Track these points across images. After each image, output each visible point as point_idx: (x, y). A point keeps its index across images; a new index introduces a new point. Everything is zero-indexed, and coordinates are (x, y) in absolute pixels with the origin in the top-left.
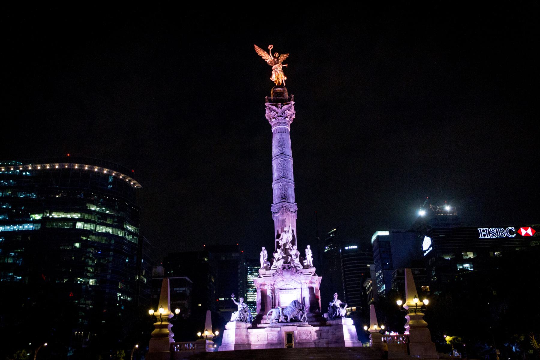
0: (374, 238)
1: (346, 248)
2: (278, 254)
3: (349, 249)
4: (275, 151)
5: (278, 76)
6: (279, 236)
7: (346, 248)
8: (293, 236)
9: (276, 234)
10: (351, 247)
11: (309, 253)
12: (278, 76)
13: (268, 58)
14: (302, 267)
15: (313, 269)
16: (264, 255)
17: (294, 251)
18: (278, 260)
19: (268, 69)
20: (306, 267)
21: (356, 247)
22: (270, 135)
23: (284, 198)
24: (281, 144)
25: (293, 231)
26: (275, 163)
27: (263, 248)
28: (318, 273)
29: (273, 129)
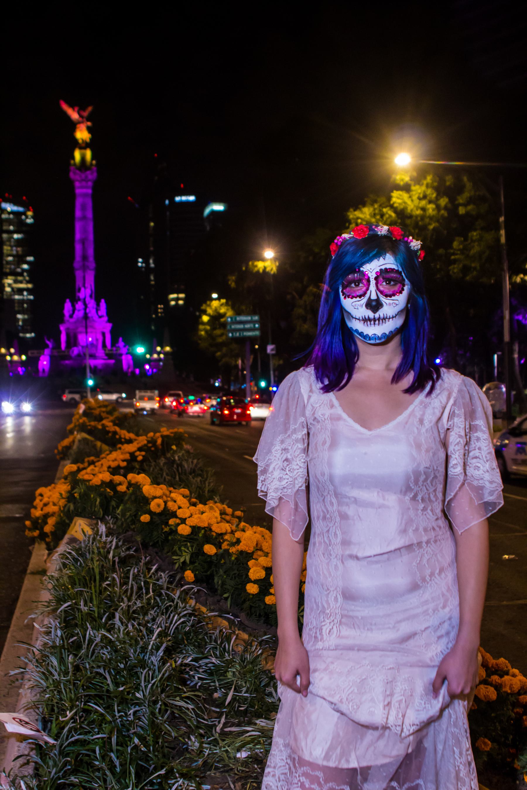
0: (207, 211)
1: (178, 199)
2: (79, 305)
3: (182, 203)
4: (78, 213)
5: (82, 134)
6: (79, 290)
7: (178, 199)
8: (92, 290)
9: (77, 288)
10: (184, 198)
11: (103, 304)
12: (82, 134)
13: (75, 116)
14: (97, 316)
15: (106, 319)
16: (68, 305)
17: (91, 303)
18: (79, 310)
19: (73, 126)
20: (100, 317)
21: (192, 198)
22: (73, 196)
23: (85, 258)
24: (84, 208)
25: (91, 286)
26: (78, 226)
27: (68, 300)
28: (109, 321)
29: (78, 191)
